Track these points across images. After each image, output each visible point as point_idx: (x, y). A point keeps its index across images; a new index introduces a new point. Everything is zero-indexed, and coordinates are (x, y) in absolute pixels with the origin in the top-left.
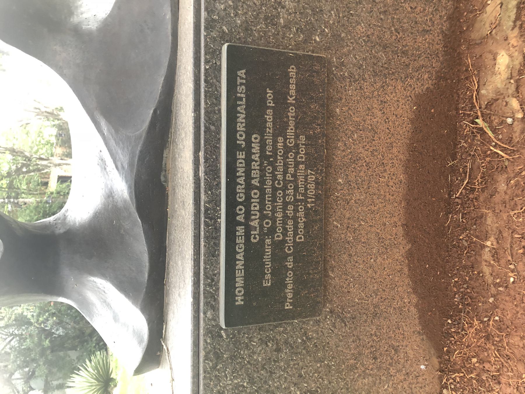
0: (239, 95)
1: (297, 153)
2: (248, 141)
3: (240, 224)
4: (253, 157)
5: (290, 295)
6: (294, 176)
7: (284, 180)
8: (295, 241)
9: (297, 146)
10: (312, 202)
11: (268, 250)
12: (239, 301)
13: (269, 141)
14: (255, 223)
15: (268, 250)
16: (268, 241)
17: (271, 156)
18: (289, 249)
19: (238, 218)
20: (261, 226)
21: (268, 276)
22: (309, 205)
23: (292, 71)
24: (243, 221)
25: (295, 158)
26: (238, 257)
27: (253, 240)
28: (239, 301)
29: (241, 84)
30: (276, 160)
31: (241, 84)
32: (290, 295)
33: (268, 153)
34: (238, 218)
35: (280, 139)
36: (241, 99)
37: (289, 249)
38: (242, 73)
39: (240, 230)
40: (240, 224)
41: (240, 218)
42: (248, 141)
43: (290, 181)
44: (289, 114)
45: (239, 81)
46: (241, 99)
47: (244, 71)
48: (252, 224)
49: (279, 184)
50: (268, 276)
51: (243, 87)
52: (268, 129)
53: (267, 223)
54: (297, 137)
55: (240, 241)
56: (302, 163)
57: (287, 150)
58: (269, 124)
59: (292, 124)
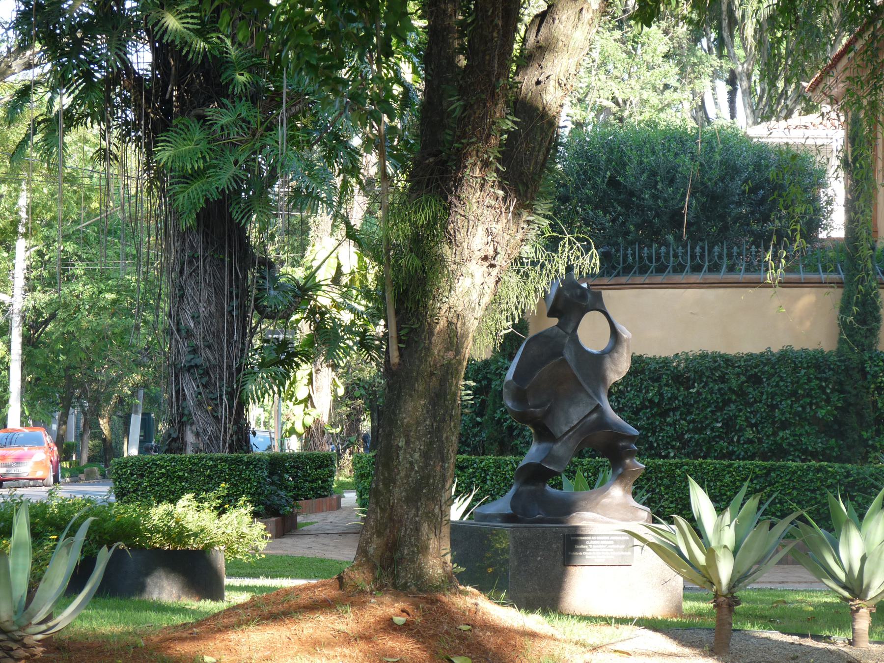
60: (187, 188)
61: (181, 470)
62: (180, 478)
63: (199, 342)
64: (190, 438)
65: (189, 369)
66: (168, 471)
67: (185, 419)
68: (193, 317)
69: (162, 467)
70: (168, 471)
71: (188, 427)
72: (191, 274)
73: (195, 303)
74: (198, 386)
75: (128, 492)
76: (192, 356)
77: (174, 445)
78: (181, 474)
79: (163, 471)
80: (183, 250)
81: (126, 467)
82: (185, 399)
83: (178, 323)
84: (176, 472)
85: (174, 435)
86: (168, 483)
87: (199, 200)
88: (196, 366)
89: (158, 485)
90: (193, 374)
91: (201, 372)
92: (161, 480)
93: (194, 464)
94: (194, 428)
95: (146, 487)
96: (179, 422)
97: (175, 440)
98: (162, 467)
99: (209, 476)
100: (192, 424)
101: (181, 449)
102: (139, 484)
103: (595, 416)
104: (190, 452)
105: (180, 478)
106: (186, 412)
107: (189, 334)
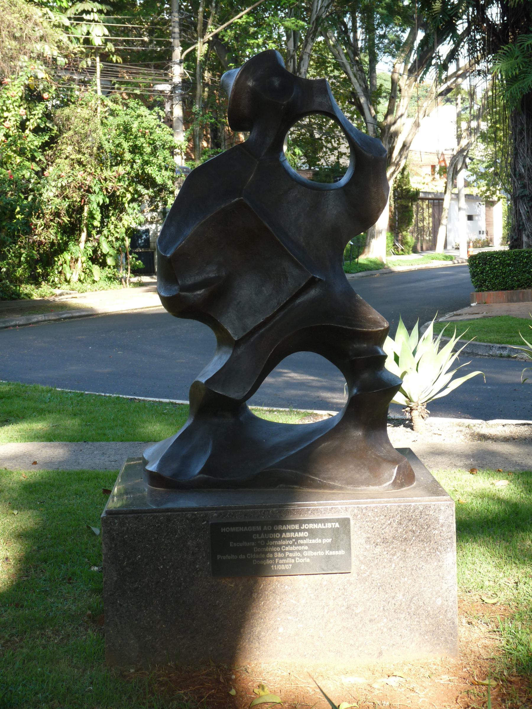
0: (326, 524)
1: (300, 557)
2: (305, 530)
3: (262, 528)
4: (296, 533)
5: (224, 557)
6: (288, 557)
7: (285, 551)
8: (253, 559)
9: (304, 557)
10: (274, 568)
11: (248, 544)
12: (223, 530)
13: (305, 542)
14: (262, 536)
15: (248, 544)
16: (253, 544)
17: (297, 543)
18: (249, 556)
19: (265, 527)
20: (261, 540)
21: (235, 545)
22: (272, 566)
23: (342, 552)
24: (264, 529)
25: (297, 557)
26: (246, 528)
27: (254, 535)
28: (223, 530)
29: (332, 525)
30: (296, 546)
31: (332, 525)
32: (224, 557)
33: (299, 541)
34: (265, 527)
35: (306, 548)
36: (325, 525)
37: (249, 556)
38: (337, 525)
39: (259, 528)
40: (262, 528)
41: (265, 528)
42: (305, 530)
43: (285, 555)
44: (320, 552)
45: (333, 524)
46: (325, 525)
47: (338, 526)
48: (262, 534)
49: (284, 548)
50: (235, 545)
51: (331, 527)
52: (311, 540)
53: (263, 543)
54: (307, 557)
55: (254, 529)
56: (295, 561)
57: (301, 551)
58: (314, 541)
59: (315, 554)
60: (510, 87)
61: (509, 260)
62: (509, 265)
63: (526, 181)
64: (525, 239)
65: (522, 197)
66: (501, 260)
67: (521, 228)
68: (523, 166)
69: (497, 258)
70: (501, 260)
71: (524, 232)
72: (521, 140)
73: (524, 157)
74: (527, 208)
75: (478, 274)
76: (523, 190)
77: (516, 243)
78: (508, 262)
79: (498, 260)
80: (516, 126)
81: (476, 259)
82: (521, 216)
83: (515, 170)
84: (505, 261)
85: (515, 237)
86: (501, 268)
87: (517, 94)
88: (525, 195)
89: (495, 269)
90: (524, 200)
91: (529, 199)
92: (497, 266)
93: (516, 256)
94: (526, 233)
95: (488, 271)
96: (518, 229)
97: (516, 240)
98: (497, 258)
99: (526, 262)
100: (525, 230)
101: (520, 246)
102: (484, 269)
103: (313, 293)
104: (525, 248)
105: (509, 265)
106: (521, 223)
107: (521, 176)
